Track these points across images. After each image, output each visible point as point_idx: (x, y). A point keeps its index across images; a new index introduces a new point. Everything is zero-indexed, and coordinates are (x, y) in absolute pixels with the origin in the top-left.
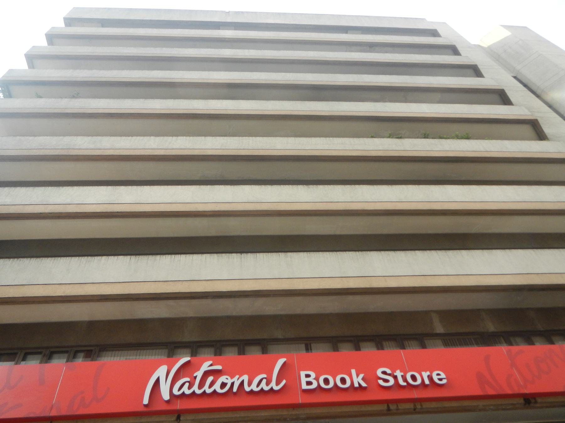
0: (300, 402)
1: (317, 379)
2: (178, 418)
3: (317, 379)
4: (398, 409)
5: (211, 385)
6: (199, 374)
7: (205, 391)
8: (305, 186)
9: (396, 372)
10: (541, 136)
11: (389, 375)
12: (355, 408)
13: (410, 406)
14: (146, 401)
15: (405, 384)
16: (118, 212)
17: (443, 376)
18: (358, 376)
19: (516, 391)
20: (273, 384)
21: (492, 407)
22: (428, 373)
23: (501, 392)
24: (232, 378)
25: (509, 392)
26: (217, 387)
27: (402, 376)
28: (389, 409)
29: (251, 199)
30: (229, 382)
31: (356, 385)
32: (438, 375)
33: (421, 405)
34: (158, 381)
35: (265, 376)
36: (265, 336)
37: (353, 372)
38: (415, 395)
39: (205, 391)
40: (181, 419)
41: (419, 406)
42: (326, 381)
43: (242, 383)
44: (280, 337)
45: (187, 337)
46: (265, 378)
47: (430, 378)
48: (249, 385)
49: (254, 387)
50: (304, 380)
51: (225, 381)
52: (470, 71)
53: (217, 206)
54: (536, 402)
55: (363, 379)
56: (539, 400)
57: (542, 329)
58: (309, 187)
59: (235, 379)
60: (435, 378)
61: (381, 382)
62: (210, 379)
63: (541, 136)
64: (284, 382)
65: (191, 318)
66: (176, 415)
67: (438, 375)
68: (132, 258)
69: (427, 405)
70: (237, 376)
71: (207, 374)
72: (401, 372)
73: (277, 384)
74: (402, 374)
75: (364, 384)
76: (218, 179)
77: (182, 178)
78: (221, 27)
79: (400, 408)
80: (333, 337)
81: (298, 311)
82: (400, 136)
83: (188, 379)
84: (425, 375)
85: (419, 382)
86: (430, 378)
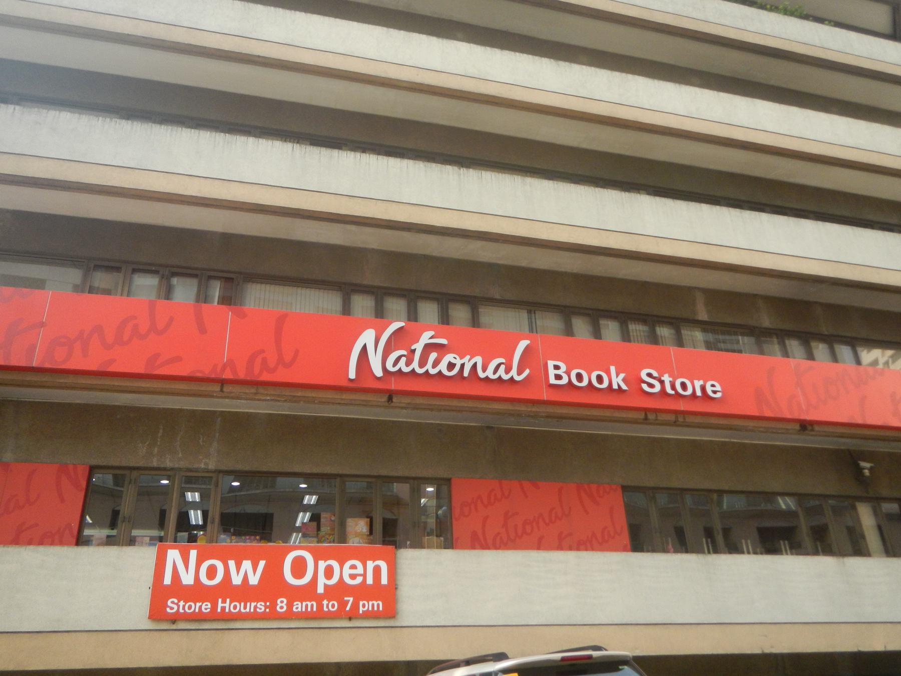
0: (545, 399)
1: (568, 373)
2: (390, 399)
3: (568, 373)
4: (656, 420)
5: (435, 364)
6: (419, 347)
7: (427, 370)
8: (552, 60)
9: (663, 376)
11: (654, 378)
12: (608, 413)
14: (352, 375)
15: (673, 392)
16: (259, 56)
17: (718, 388)
18: (617, 375)
19: (796, 416)
20: (514, 373)
21: (761, 429)
22: (701, 382)
23: (779, 415)
24: (461, 358)
25: (789, 416)
26: (443, 367)
27: (670, 381)
28: (646, 418)
29: (472, 71)
30: (458, 362)
31: (615, 387)
32: (713, 386)
33: (684, 419)
34: (364, 348)
35: (503, 360)
36: (477, 292)
37: (613, 369)
38: (682, 406)
39: (427, 371)
40: (394, 400)
41: (681, 419)
42: (579, 377)
43: (475, 365)
44: (498, 297)
45: (369, 279)
46: (503, 363)
47: (703, 388)
48: (484, 370)
49: (489, 373)
50: (552, 372)
51: (453, 361)
53: (418, 75)
54: (813, 430)
55: (624, 380)
56: (817, 428)
57: (826, 333)
60: (709, 389)
61: (645, 387)
62: (433, 356)
64: (527, 372)
65: (373, 251)
66: (387, 396)
67: (713, 386)
68: (294, 147)
69: (690, 419)
70: (468, 357)
71: (429, 348)
72: (670, 376)
73: (519, 374)
74: (671, 379)
75: (624, 387)
76: (400, 9)
79: (659, 418)
80: (565, 307)
81: (524, 263)
83: (404, 352)
84: (698, 384)
85: (689, 392)
86: (703, 388)
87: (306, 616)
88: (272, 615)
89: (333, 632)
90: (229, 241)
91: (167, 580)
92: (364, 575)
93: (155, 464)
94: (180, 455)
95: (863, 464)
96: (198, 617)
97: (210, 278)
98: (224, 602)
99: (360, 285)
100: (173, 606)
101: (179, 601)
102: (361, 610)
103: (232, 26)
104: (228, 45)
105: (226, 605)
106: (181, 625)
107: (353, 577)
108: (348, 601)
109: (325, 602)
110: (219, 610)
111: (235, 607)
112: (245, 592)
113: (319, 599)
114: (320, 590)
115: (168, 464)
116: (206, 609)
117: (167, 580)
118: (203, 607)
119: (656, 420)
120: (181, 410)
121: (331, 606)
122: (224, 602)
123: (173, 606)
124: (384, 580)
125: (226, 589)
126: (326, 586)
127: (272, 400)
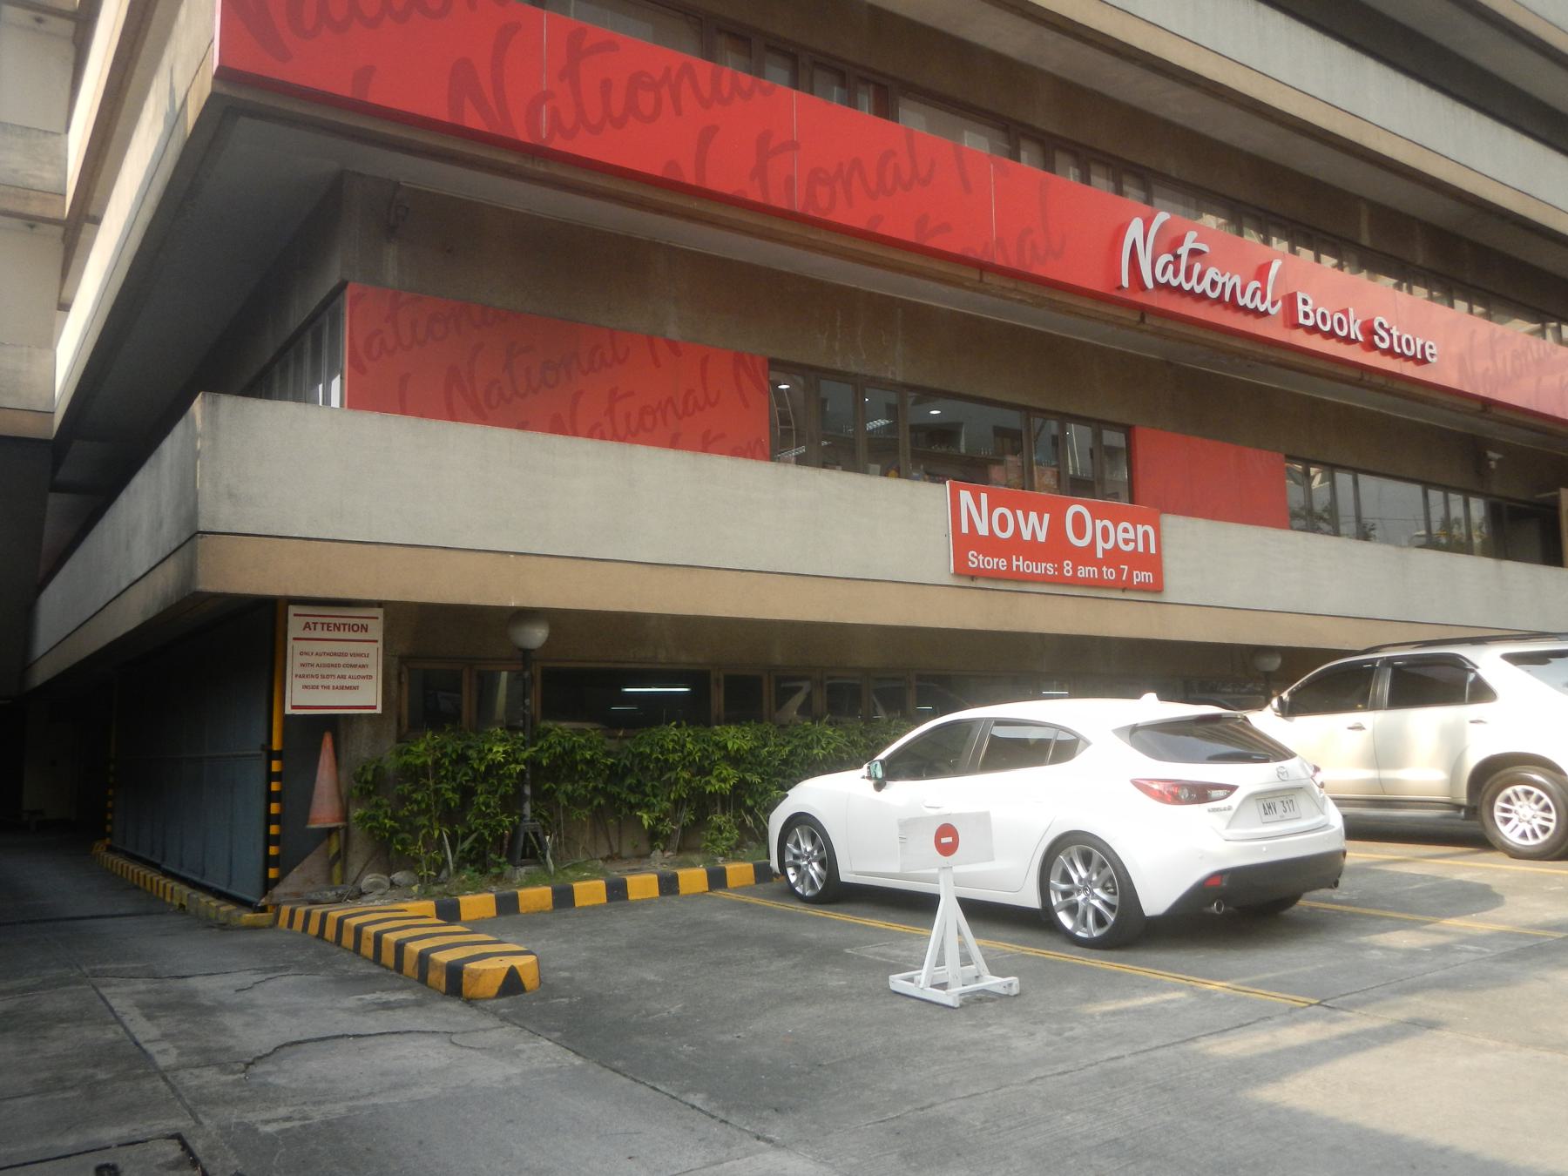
13: (1355, 374)
20: (1268, 303)
44: (1174, 174)
56: (1494, 410)
59: (1226, 278)
87: (1088, 583)
88: (1059, 580)
89: (1110, 603)
91: (965, 529)
92: (1135, 541)
93: (839, 366)
94: (864, 357)
95: (1491, 454)
96: (994, 576)
97: (866, 81)
98: (1018, 560)
99: (1032, 128)
100: (975, 560)
101: (978, 555)
102: (1135, 581)
105: (1019, 564)
106: (981, 583)
107: (1126, 542)
108: (1124, 569)
109: (1104, 569)
110: (1014, 569)
111: (1028, 567)
112: (1032, 550)
113: (1098, 564)
114: (1100, 555)
115: (854, 368)
116: (1003, 566)
117: (965, 529)
118: (1000, 564)
119: (1361, 380)
120: (856, 290)
121: (1109, 573)
122: (1018, 560)
123: (975, 560)
124: (1153, 551)
125: (1017, 546)
126: (1104, 550)
127: (1021, 301)
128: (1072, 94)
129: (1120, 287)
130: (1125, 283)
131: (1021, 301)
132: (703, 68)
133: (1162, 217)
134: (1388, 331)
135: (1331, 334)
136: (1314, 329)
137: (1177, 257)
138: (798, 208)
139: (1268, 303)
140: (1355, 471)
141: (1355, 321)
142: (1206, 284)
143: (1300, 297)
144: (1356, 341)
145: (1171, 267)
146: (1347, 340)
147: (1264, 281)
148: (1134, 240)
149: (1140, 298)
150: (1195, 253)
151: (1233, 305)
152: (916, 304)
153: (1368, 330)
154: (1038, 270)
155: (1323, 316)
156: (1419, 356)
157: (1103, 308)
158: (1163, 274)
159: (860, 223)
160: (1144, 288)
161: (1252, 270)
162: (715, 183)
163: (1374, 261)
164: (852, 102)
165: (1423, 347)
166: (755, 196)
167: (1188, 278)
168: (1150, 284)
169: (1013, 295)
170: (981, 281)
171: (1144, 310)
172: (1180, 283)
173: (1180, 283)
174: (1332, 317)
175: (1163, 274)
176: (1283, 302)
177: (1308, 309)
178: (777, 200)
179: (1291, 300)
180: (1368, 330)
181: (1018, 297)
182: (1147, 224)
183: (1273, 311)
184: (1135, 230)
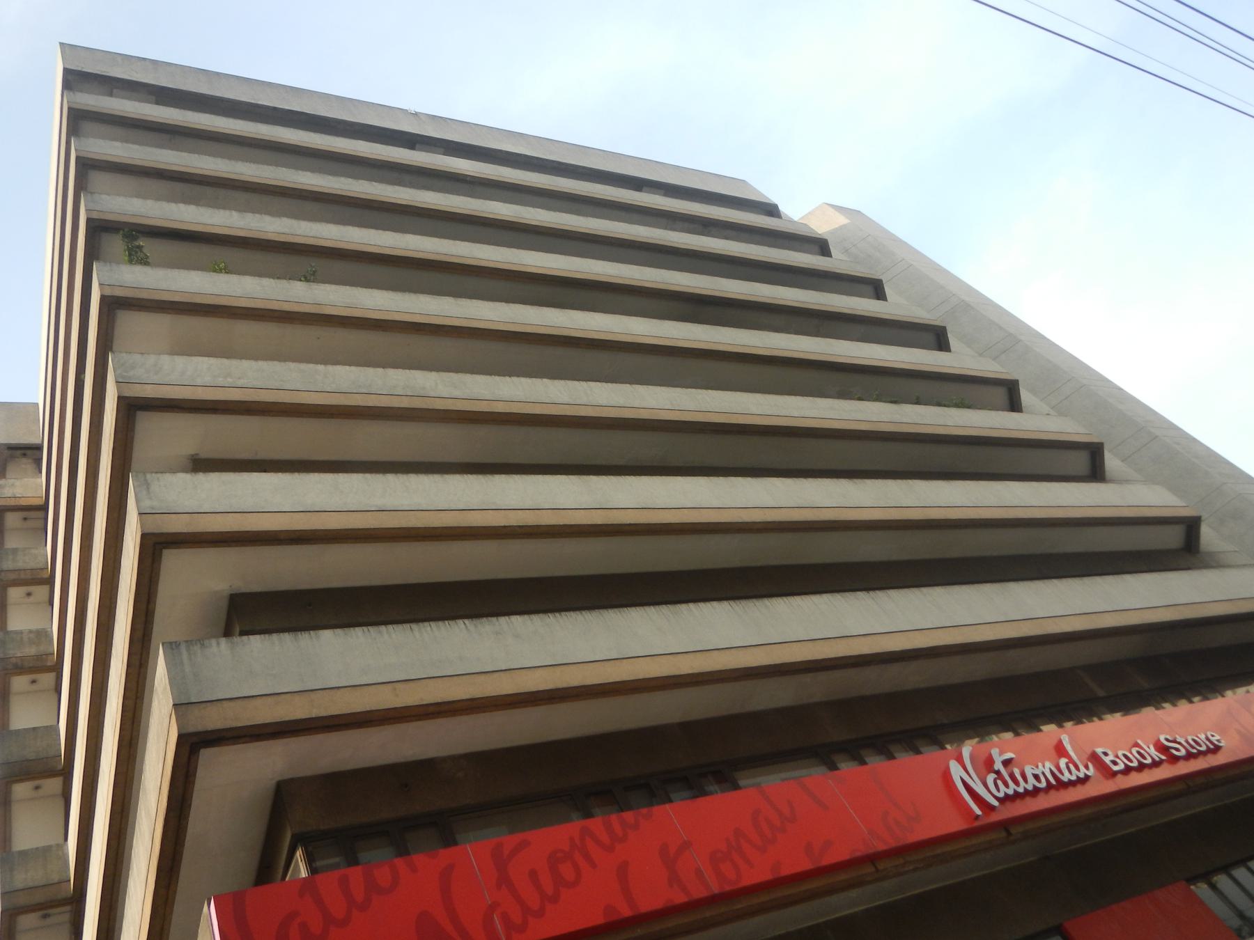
10: (1014, 405)
13: (1180, 786)
16: (630, 525)
20: (1082, 768)
44: (945, 721)
52: (870, 289)
58: (855, 483)
63: (1014, 405)
77: (599, 462)
78: (417, 146)
82: (895, 399)
90: (691, 731)
103: (586, 500)
104: (598, 519)
128: (845, 708)
129: (977, 817)
130: (978, 812)
131: (915, 870)
132: (596, 824)
133: (966, 751)
134: (1175, 741)
135: (1141, 767)
136: (1127, 770)
137: (998, 773)
138: (716, 889)
139: (1082, 768)
140: (1243, 862)
141: (1149, 747)
142: (1031, 780)
143: (1099, 751)
144: (1161, 762)
145: (999, 782)
146: (1156, 764)
147: (1066, 755)
148: (961, 777)
149: (994, 817)
150: (1007, 763)
151: (1062, 785)
152: (837, 919)
153: (1163, 749)
154: (912, 838)
155: (1125, 756)
156: (1212, 747)
157: (975, 841)
158: (998, 790)
159: (768, 876)
160: (992, 808)
161: (1053, 753)
162: (646, 905)
163: (1128, 702)
164: (703, 793)
165: (1208, 739)
166: (680, 898)
167: (1017, 783)
168: (996, 803)
169: (906, 869)
170: (877, 870)
171: (1005, 825)
172: (1014, 790)
173: (1014, 790)
174: (1131, 753)
175: (998, 790)
176: (1091, 762)
177: (1111, 757)
178: (699, 893)
179: (1095, 758)
180: (1163, 749)
181: (911, 868)
182: (960, 760)
183: (1089, 773)
184: (956, 771)
